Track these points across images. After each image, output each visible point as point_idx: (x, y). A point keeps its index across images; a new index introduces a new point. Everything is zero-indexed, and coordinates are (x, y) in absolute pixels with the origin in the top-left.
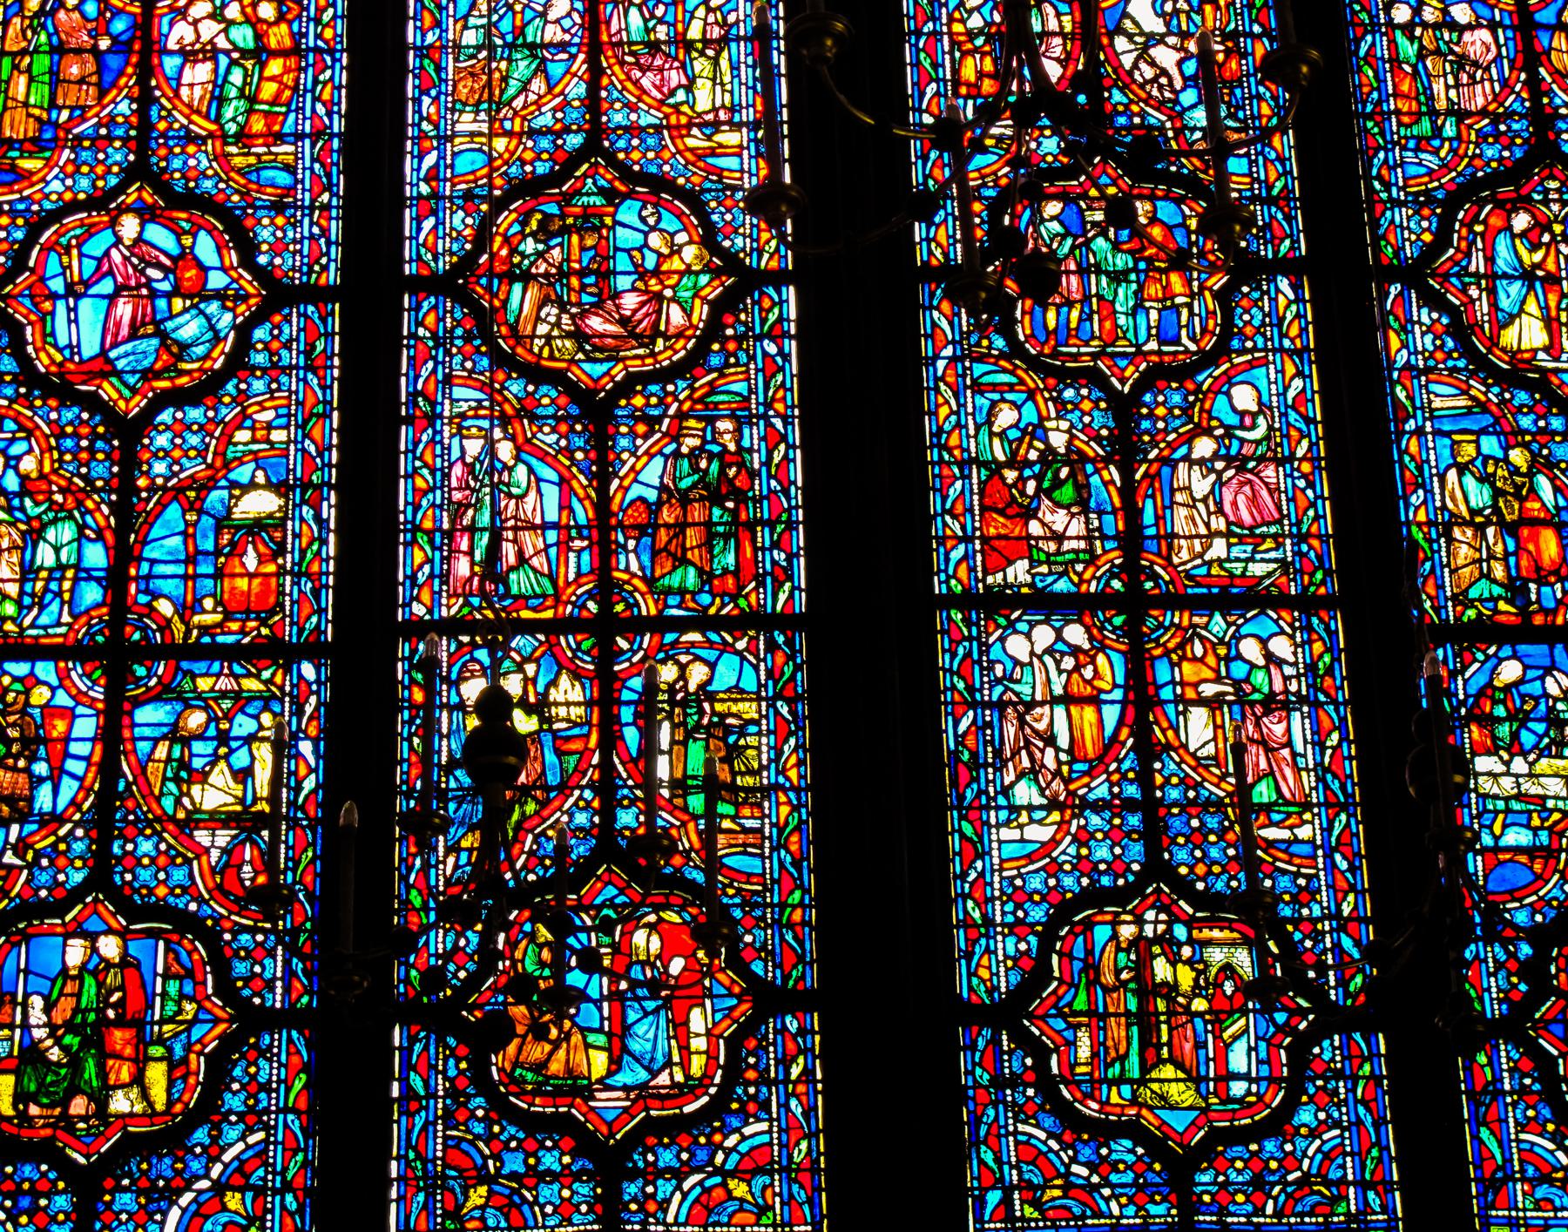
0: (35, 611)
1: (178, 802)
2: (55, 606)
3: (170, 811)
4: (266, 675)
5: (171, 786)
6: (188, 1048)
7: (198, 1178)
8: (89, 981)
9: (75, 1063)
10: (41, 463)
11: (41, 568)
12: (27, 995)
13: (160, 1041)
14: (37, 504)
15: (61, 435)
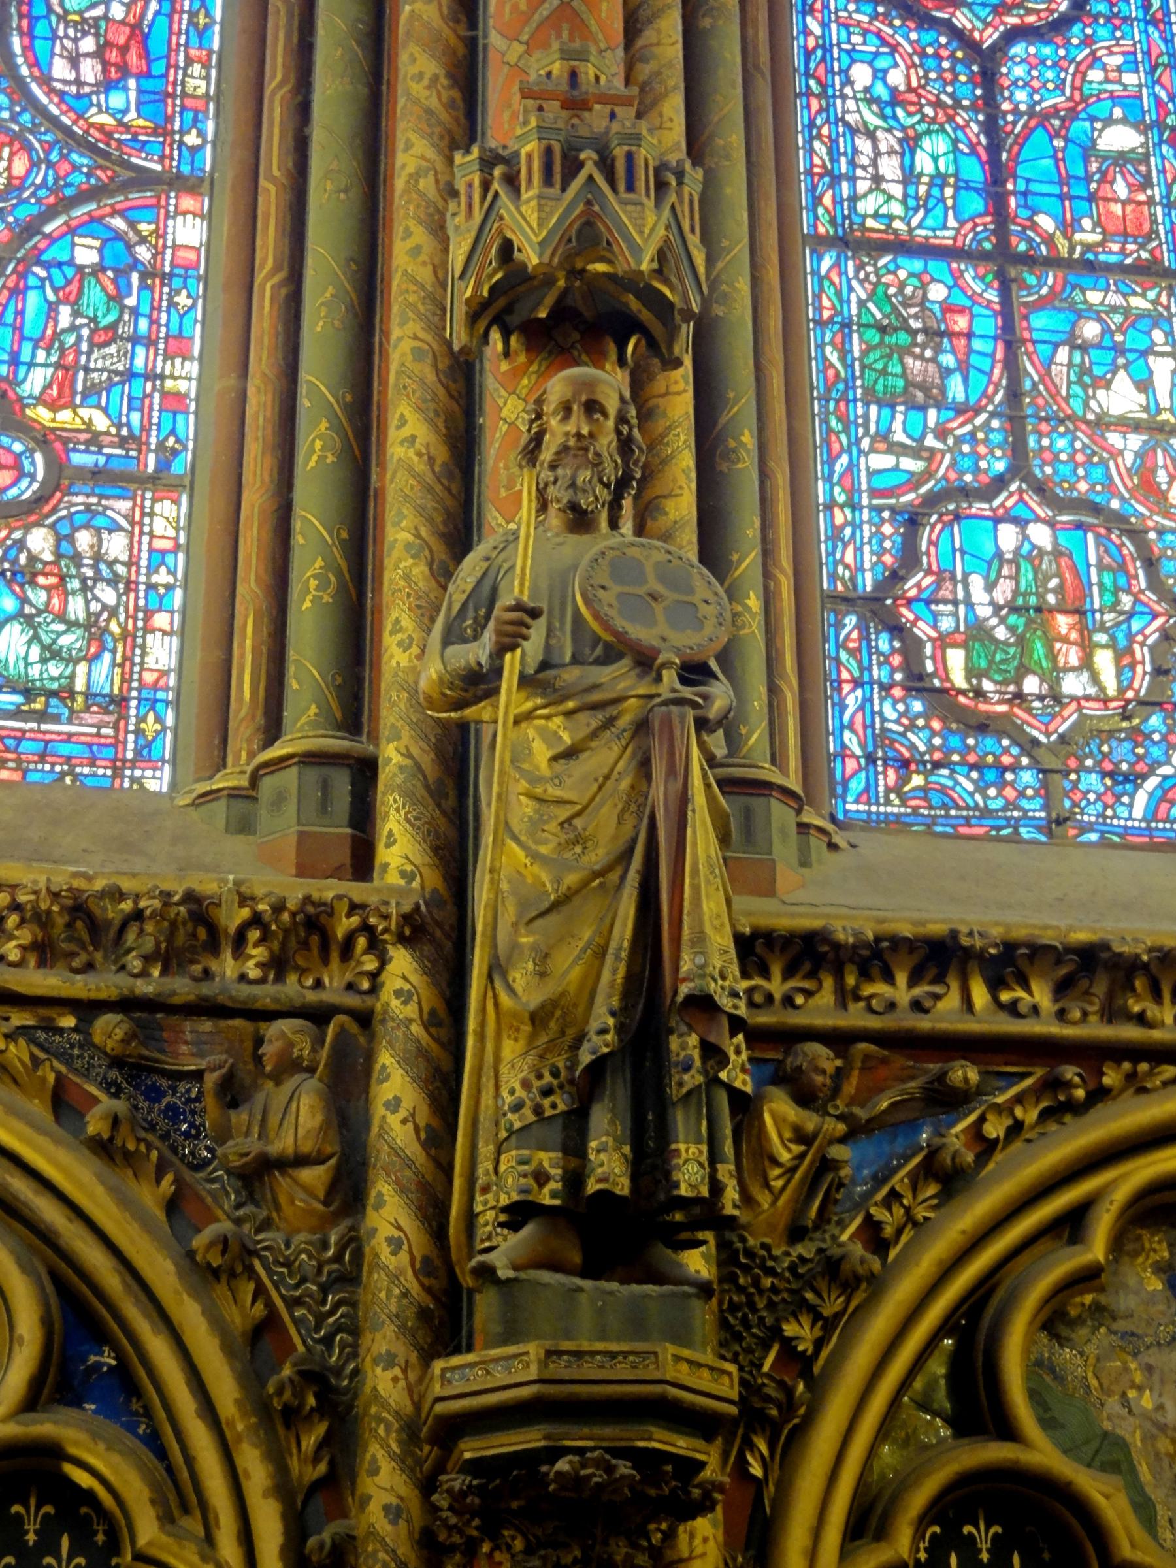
0: (921, 212)
1: (1086, 406)
2: (939, 210)
3: (1080, 413)
4: (1152, 295)
5: (1076, 389)
6: (1131, 638)
7: (1160, 764)
8: (1025, 566)
9: (1021, 641)
10: (908, 77)
11: (921, 174)
12: (966, 576)
13: (1103, 628)
14: (910, 114)
15: (923, 54)
